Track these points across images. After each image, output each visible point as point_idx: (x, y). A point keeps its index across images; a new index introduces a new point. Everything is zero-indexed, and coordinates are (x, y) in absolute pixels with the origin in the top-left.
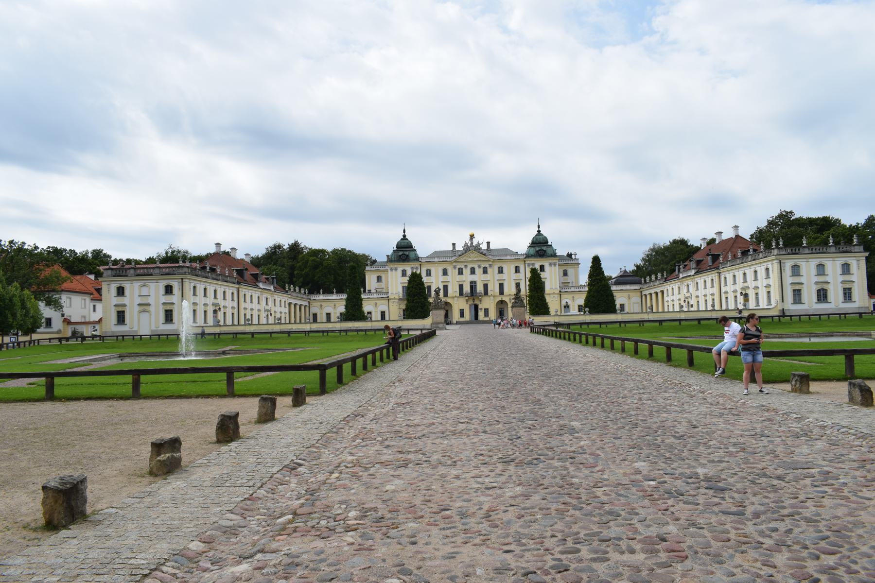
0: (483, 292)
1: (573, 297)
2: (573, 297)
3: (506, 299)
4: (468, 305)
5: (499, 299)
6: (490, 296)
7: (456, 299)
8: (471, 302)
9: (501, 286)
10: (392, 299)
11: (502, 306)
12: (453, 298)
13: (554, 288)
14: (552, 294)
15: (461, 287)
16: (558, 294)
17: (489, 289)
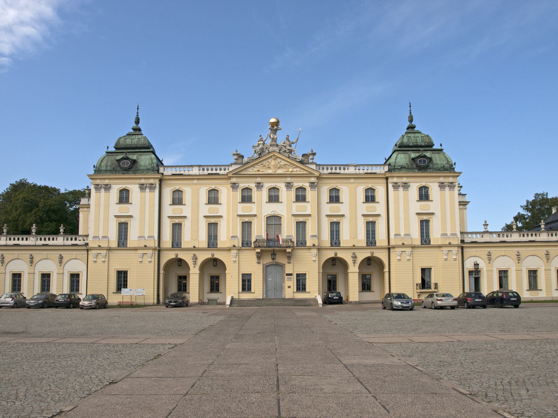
0: (294, 240)
1: (489, 255)
2: (489, 255)
3: (346, 256)
4: (260, 267)
5: (330, 254)
6: (309, 248)
7: (234, 252)
8: (268, 260)
9: (335, 227)
10: (95, 249)
11: (332, 271)
12: (229, 250)
13: (449, 233)
14: (445, 246)
15: (247, 226)
16: (458, 247)
17: (311, 230)
